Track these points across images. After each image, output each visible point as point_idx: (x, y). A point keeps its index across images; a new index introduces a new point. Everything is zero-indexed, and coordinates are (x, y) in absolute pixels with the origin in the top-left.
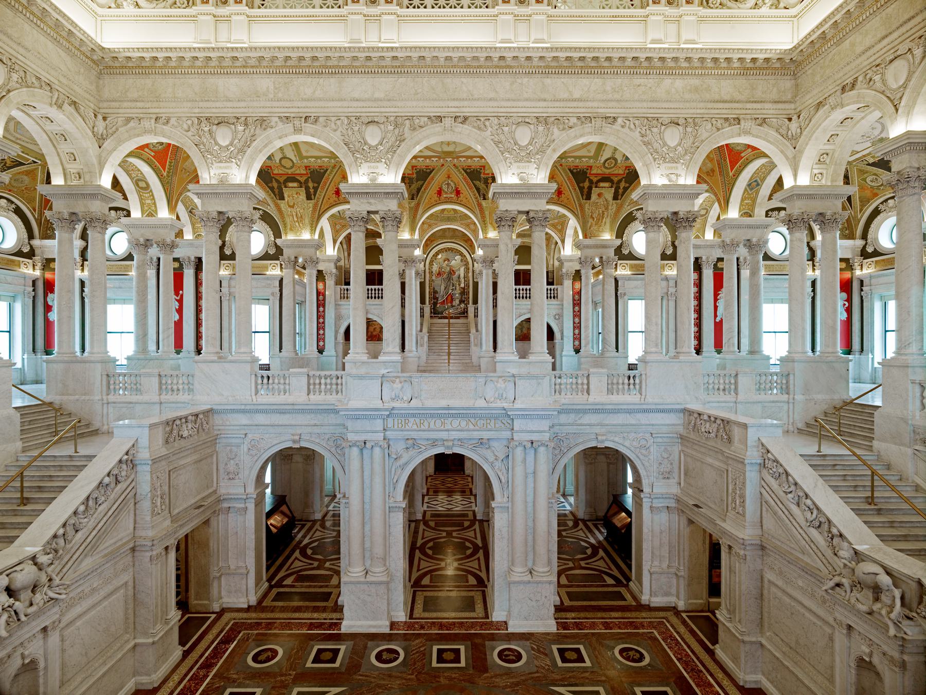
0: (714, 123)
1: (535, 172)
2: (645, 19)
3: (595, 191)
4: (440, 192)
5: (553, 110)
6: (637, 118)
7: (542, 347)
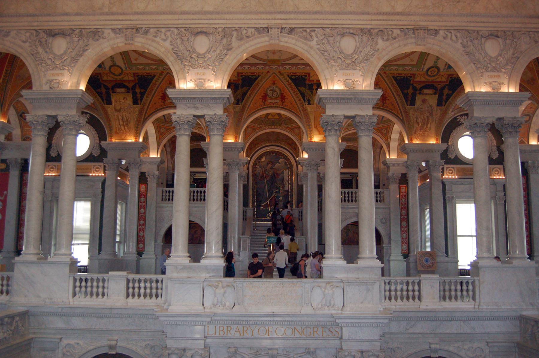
0: (533, 36)
1: (361, 79)
3: (419, 99)
4: (265, 97)
5: (375, 22)
6: (458, 31)
7: (371, 252)
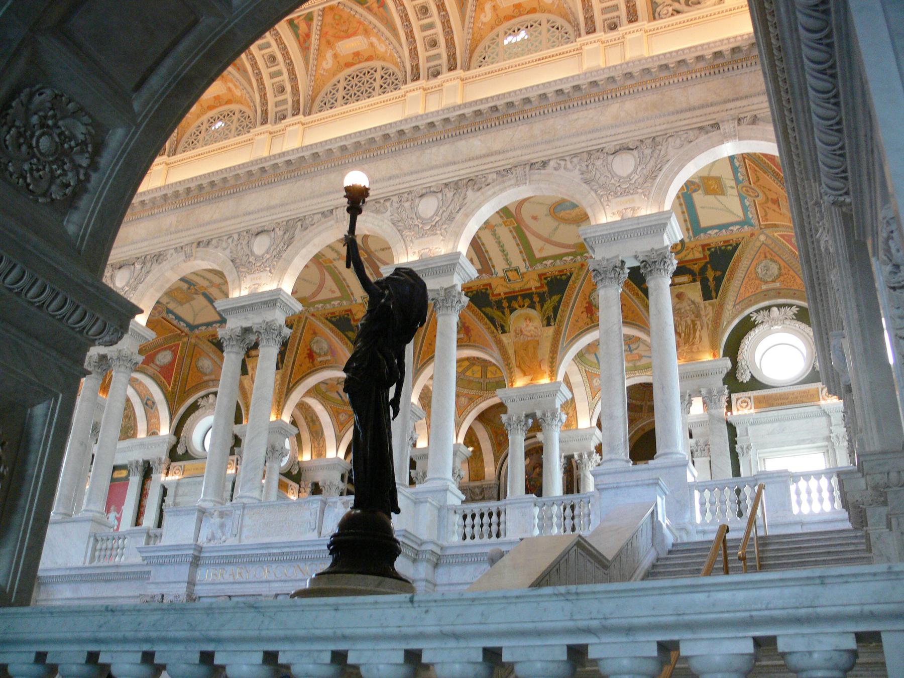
2: (579, 52)
6: (575, 155)
